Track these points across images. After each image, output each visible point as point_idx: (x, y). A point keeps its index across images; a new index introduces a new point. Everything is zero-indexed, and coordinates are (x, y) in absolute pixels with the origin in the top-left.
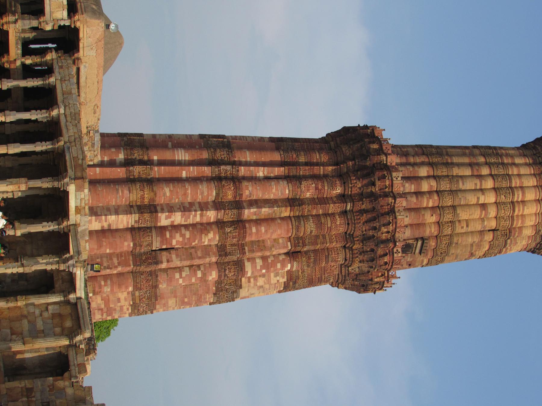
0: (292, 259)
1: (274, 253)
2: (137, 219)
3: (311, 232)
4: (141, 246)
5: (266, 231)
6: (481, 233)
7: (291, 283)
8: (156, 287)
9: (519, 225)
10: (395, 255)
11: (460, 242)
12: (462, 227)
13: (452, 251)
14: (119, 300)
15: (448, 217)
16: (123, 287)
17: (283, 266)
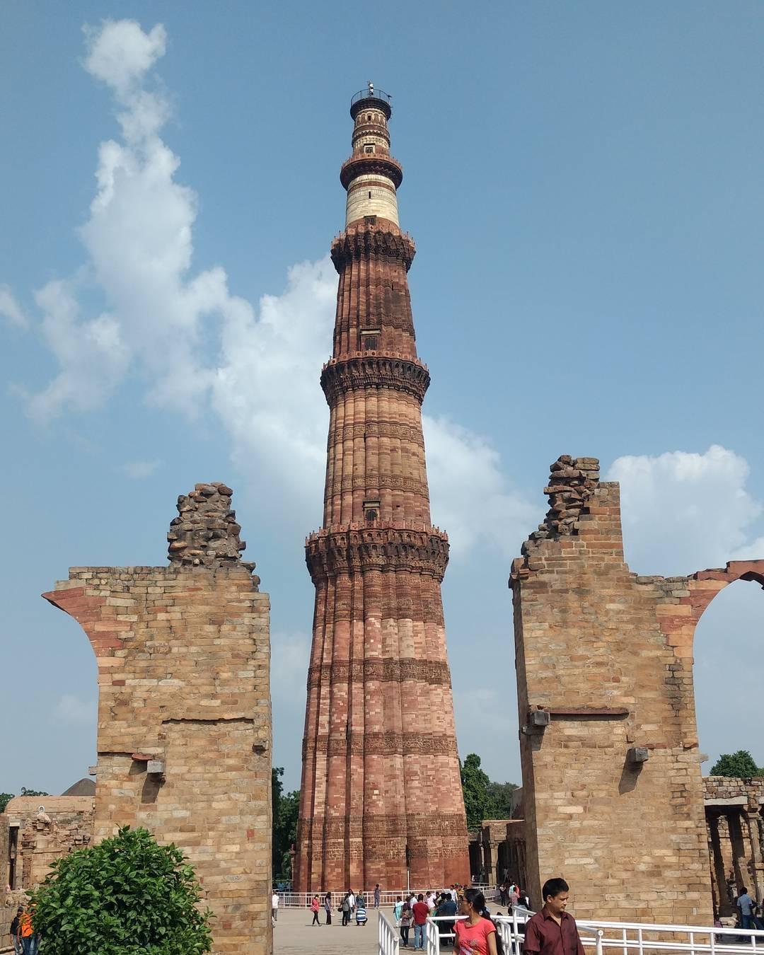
0: (366, 617)
1: (362, 633)
2: (321, 753)
3: (344, 604)
4: (337, 749)
5: (338, 643)
6: (366, 448)
7: (400, 612)
8: (376, 735)
9: (363, 415)
10: (364, 528)
11: (371, 468)
12: (356, 469)
13: (382, 471)
14: (392, 766)
15: (348, 484)
16: (371, 763)
17: (372, 624)
